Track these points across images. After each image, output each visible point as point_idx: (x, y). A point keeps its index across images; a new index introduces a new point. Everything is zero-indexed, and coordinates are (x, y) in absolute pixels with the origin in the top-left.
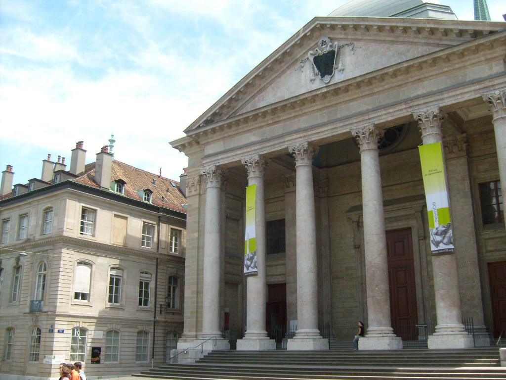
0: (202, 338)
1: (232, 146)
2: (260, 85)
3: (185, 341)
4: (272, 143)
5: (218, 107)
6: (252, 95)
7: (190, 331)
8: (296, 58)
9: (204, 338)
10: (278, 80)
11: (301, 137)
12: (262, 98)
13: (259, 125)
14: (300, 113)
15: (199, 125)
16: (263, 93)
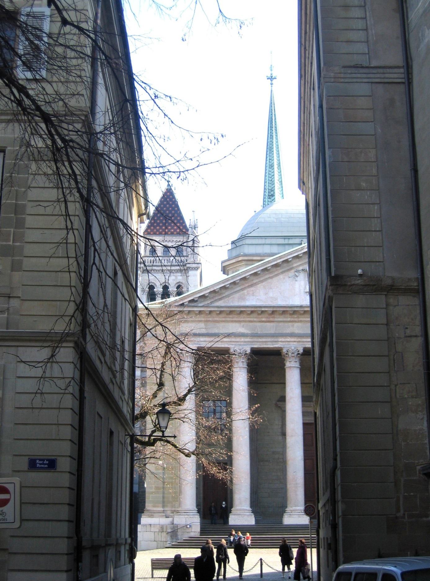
0: (186, 514)
1: (216, 331)
2: (253, 280)
3: (151, 516)
4: (264, 340)
5: (209, 291)
6: (242, 287)
7: (154, 507)
8: (291, 267)
9: (188, 514)
10: (270, 281)
11: (295, 342)
12: (251, 292)
13: (252, 319)
14: (296, 320)
15: (183, 303)
16: (252, 289)
